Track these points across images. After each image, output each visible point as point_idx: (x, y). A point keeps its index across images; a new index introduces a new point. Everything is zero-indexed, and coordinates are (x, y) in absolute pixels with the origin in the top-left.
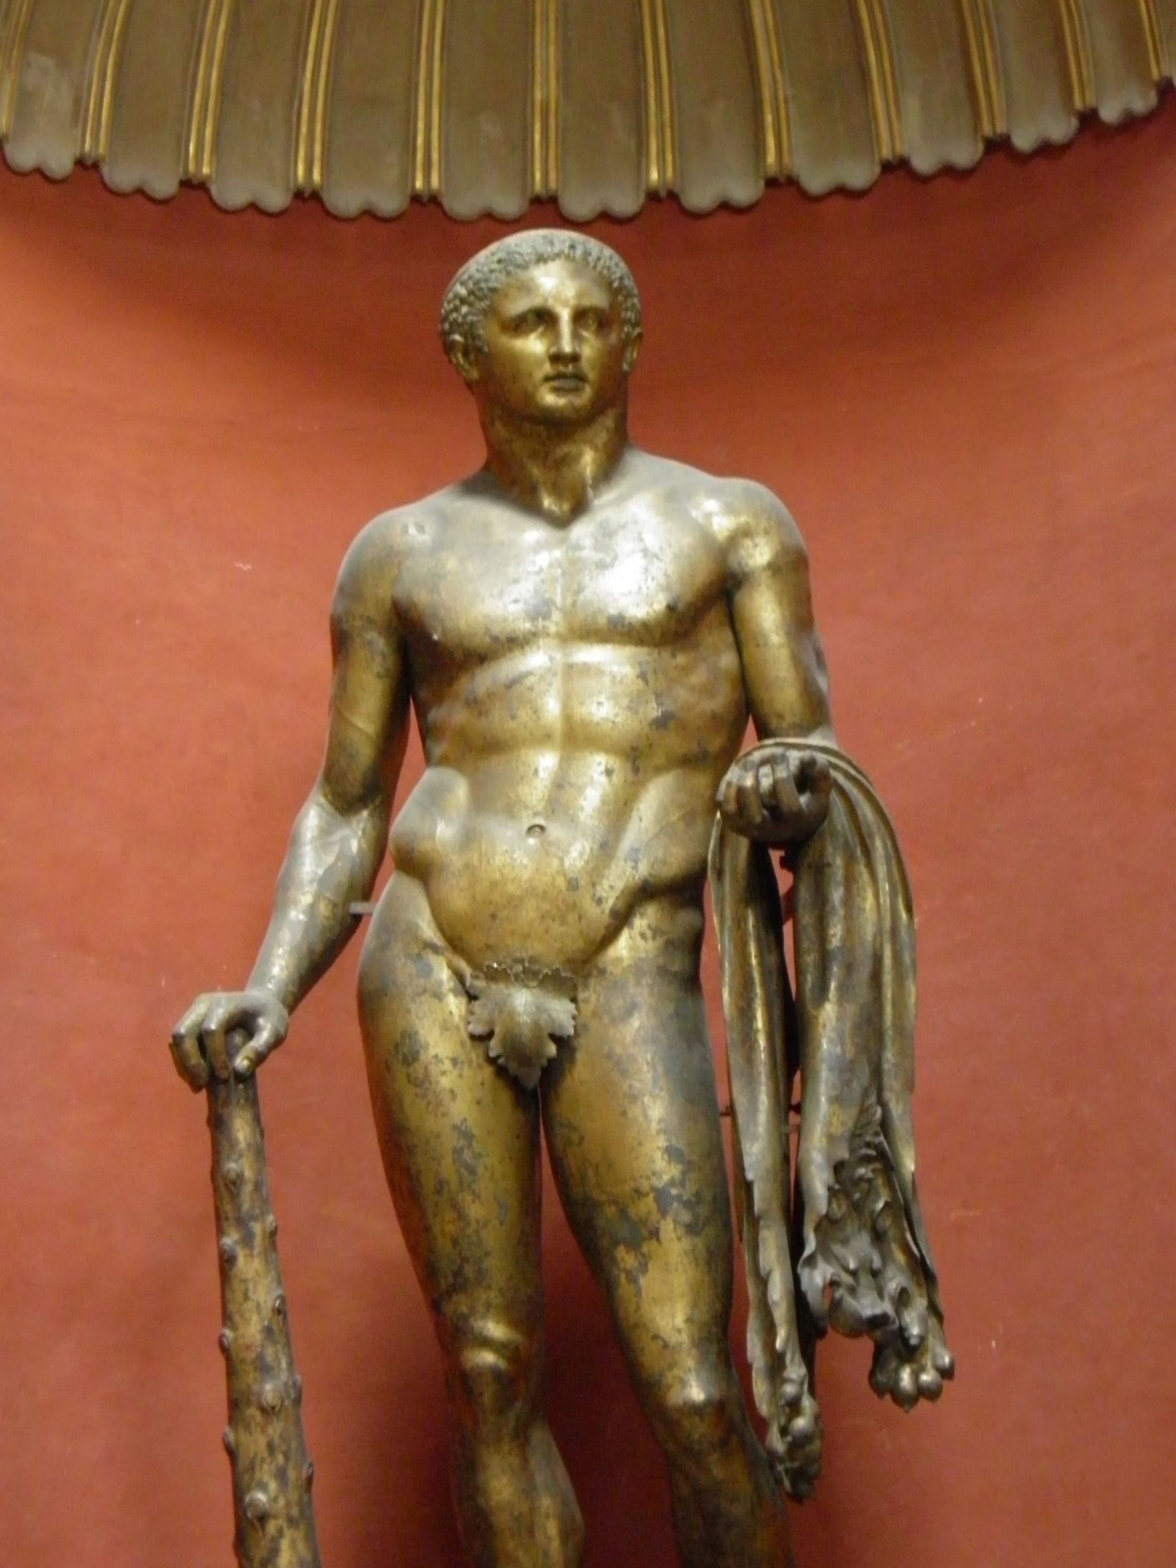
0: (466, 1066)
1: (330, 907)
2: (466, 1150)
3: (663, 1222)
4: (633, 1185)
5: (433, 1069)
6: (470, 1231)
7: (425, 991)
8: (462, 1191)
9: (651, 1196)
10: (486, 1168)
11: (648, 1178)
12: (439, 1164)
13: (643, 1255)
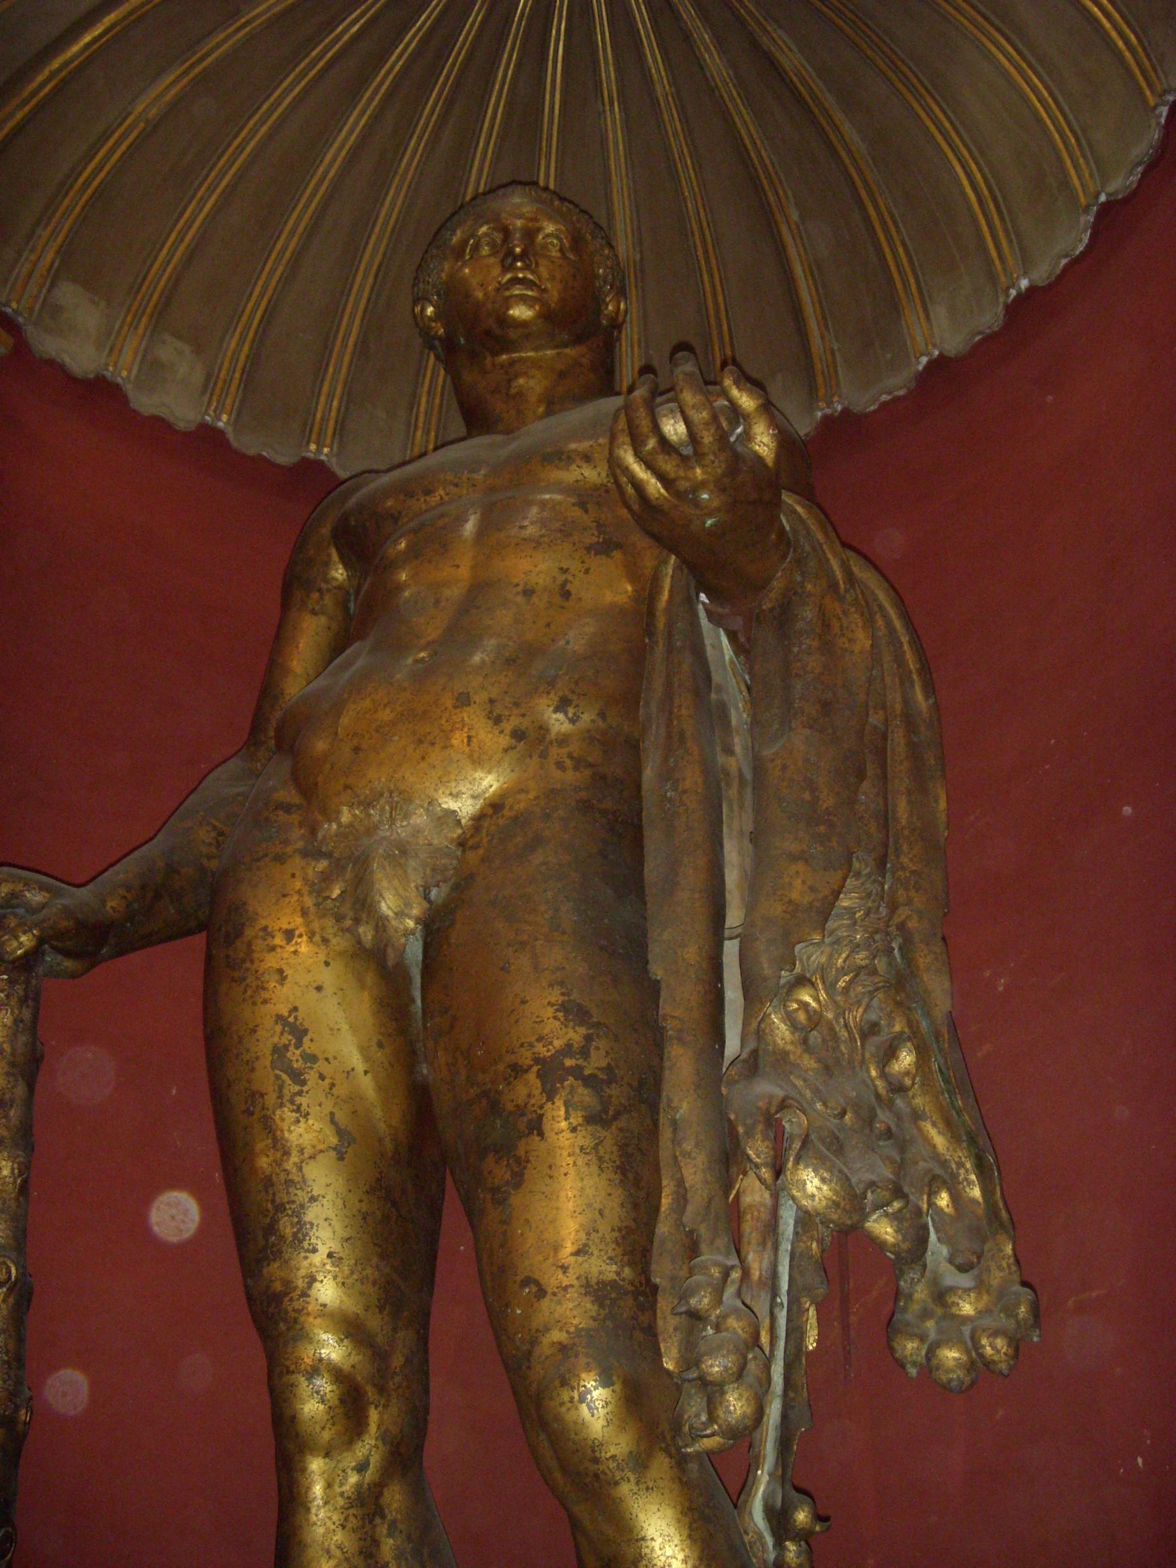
0: (305, 938)
1: (213, 834)
2: (292, 1048)
3: (549, 1104)
4: (510, 1059)
5: (259, 945)
6: (289, 1165)
7: (266, 855)
8: (282, 1105)
9: (535, 1069)
10: (322, 1077)
11: (531, 1045)
12: (253, 1070)
13: (518, 1160)
